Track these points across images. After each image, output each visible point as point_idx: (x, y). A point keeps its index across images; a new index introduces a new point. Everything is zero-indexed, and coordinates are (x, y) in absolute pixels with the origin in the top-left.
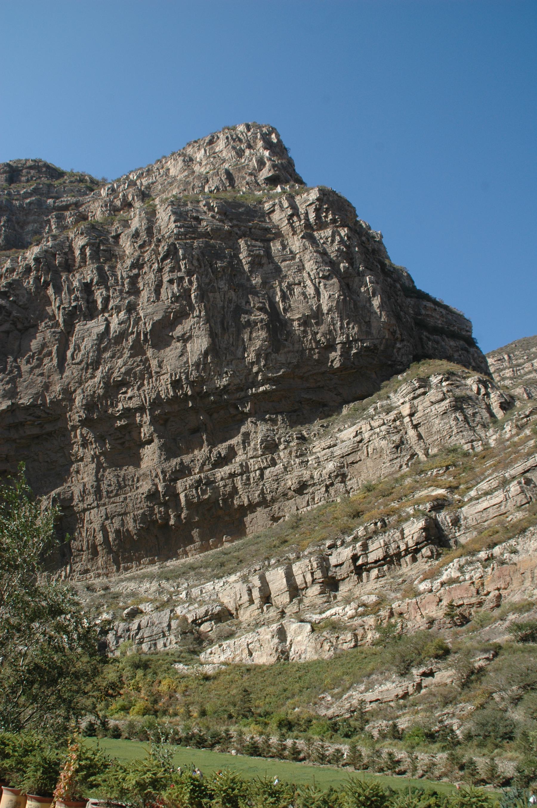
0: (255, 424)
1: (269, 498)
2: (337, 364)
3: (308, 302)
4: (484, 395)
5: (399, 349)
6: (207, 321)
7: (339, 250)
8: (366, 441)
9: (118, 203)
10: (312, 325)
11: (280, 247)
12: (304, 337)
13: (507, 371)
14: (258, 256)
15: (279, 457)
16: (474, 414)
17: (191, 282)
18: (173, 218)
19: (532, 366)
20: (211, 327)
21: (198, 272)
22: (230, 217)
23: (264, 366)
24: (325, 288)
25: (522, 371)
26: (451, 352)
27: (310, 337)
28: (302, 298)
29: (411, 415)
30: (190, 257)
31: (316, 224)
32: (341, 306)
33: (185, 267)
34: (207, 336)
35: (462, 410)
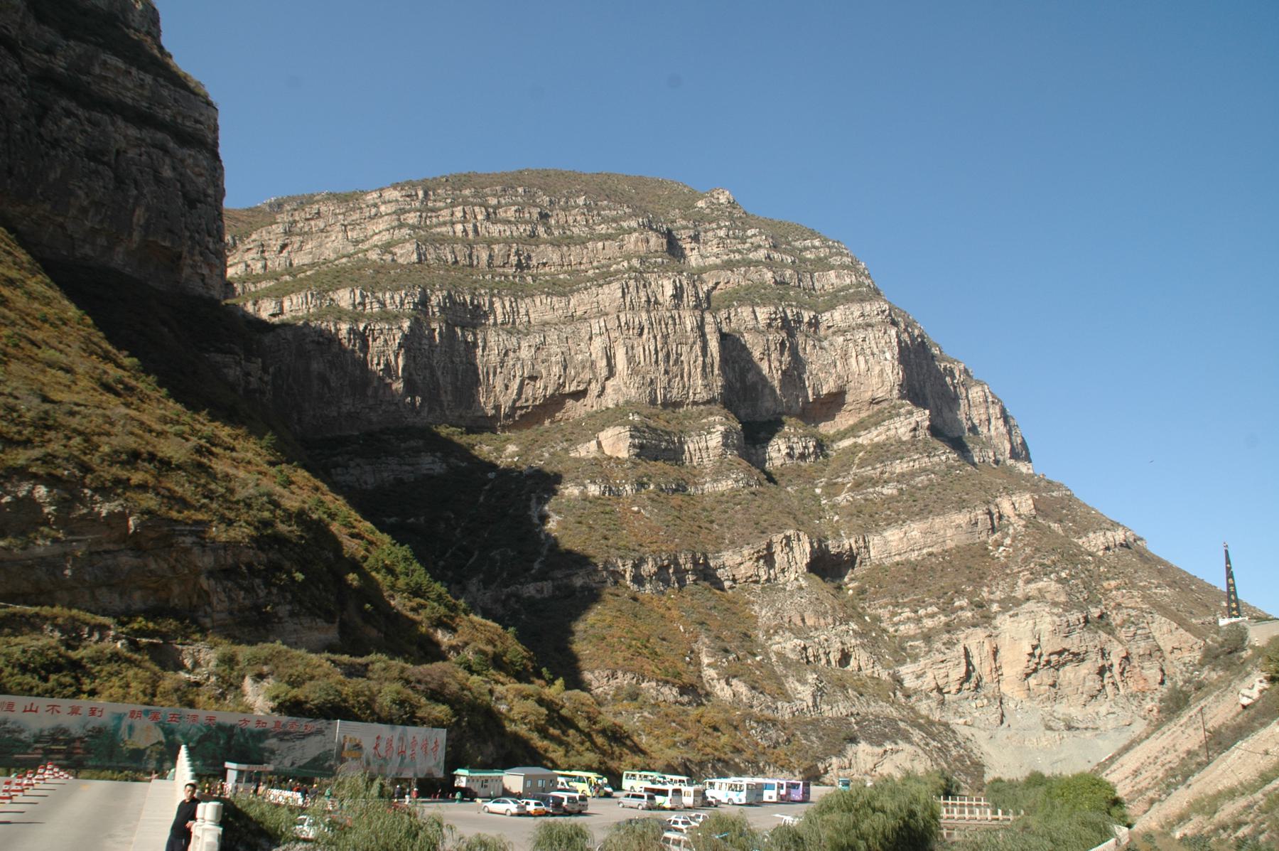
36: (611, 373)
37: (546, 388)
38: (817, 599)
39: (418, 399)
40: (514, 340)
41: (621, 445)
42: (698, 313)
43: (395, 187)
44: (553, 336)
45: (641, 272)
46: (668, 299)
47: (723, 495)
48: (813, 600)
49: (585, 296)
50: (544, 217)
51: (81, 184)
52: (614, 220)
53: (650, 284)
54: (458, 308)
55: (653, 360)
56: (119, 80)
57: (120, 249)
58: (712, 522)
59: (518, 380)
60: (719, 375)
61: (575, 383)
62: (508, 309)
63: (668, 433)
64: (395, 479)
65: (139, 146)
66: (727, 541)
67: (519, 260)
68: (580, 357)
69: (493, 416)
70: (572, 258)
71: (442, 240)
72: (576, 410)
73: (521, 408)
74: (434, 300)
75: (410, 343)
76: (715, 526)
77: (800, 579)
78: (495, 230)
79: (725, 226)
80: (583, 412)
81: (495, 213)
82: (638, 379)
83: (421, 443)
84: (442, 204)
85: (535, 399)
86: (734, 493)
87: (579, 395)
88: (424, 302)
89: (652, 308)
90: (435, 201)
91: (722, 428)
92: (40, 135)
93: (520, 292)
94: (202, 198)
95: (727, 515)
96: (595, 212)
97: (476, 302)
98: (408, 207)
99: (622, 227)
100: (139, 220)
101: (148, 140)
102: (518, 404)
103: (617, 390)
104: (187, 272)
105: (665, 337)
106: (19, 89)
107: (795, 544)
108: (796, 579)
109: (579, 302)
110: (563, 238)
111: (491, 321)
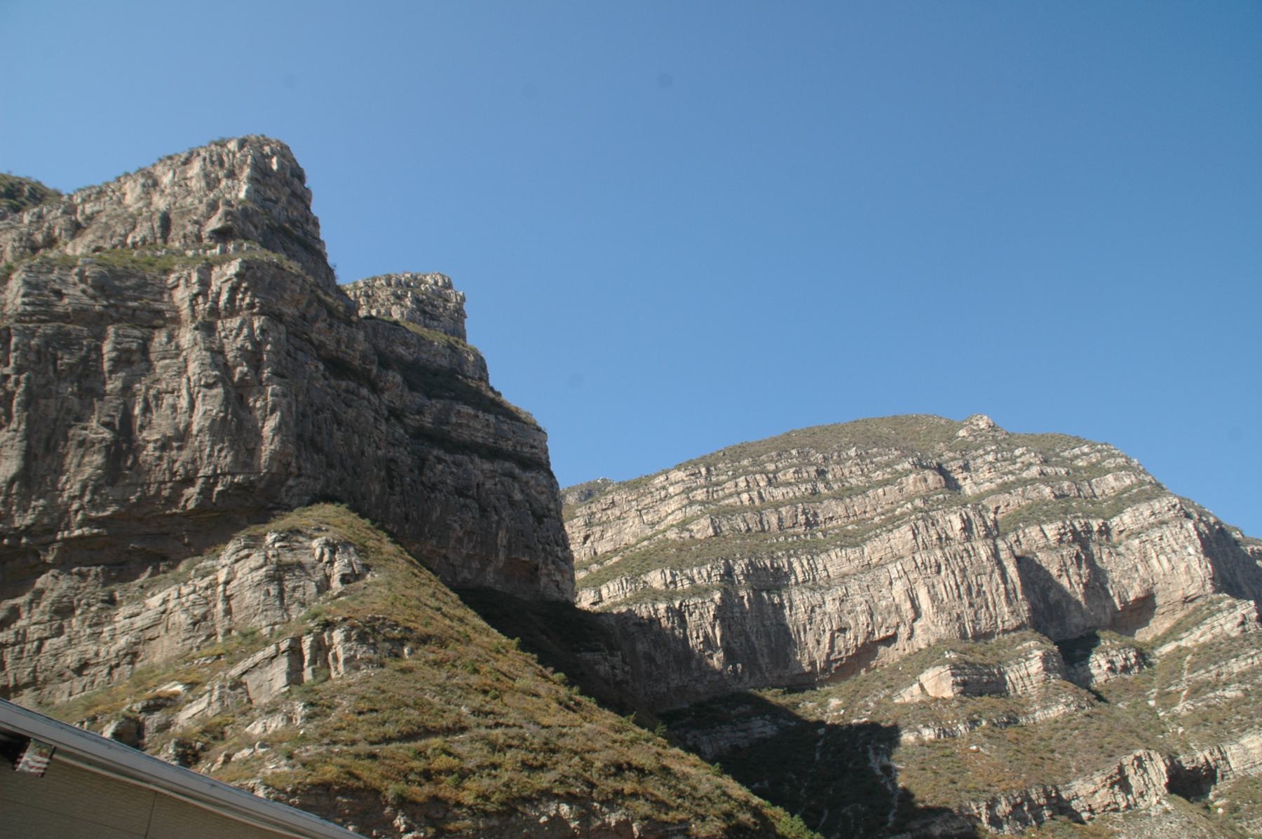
0: (56, 578)
1: (41, 678)
2: (191, 505)
3: (175, 418)
4: (327, 563)
5: (291, 487)
6: (27, 436)
7: (242, 348)
8: (168, 612)
9: (39, 237)
10: (172, 449)
11: (165, 340)
12: (157, 466)
13: (700, 491)
14: (129, 351)
15: (70, 626)
16: (294, 589)
17: (17, 383)
18: (22, 291)
19: (736, 486)
20: (29, 447)
21: (33, 370)
22: (108, 293)
23: (89, 502)
24: (204, 400)
25: (720, 493)
26: (481, 478)
27: (165, 466)
28: (169, 412)
29: (227, 583)
30: (26, 349)
31: (226, 308)
32: (216, 427)
33: (15, 363)
34: (20, 458)
35: (280, 581)
36: (917, 614)
37: (856, 638)
39: (739, 666)
40: (818, 596)
41: (944, 684)
42: (989, 541)
43: (678, 468)
44: (854, 586)
45: (926, 512)
46: (958, 533)
47: (1056, 722)
49: (877, 543)
50: (821, 473)
51: (456, 518)
52: (888, 465)
53: (938, 521)
54: (760, 573)
55: (956, 595)
56: (471, 424)
57: (490, 569)
58: (1052, 751)
59: (828, 634)
60: (1023, 599)
61: (883, 629)
62: (807, 567)
63: (986, 666)
64: (731, 746)
66: (1074, 770)
67: (807, 519)
68: (884, 603)
69: (810, 673)
70: (856, 508)
71: (731, 511)
72: (889, 656)
73: (836, 661)
74: (737, 570)
75: (725, 613)
76: (1057, 755)
78: (778, 493)
79: (992, 450)
80: (896, 657)
81: (775, 477)
82: (944, 616)
83: (749, 707)
84: (724, 478)
85: (847, 650)
86: (1068, 718)
87: (890, 640)
88: (729, 572)
89: (944, 545)
91: (1039, 653)
92: (422, 483)
93: (814, 549)
94: (547, 513)
95: (1066, 742)
96: (868, 461)
97: (776, 565)
98: (694, 485)
99: (897, 471)
102: (832, 657)
103: (926, 630)
104: (544, 580)
105: (963, 570)
107: (1147, 764)
109: (873, 550)
110: (843, 491)
111: (793, 581)
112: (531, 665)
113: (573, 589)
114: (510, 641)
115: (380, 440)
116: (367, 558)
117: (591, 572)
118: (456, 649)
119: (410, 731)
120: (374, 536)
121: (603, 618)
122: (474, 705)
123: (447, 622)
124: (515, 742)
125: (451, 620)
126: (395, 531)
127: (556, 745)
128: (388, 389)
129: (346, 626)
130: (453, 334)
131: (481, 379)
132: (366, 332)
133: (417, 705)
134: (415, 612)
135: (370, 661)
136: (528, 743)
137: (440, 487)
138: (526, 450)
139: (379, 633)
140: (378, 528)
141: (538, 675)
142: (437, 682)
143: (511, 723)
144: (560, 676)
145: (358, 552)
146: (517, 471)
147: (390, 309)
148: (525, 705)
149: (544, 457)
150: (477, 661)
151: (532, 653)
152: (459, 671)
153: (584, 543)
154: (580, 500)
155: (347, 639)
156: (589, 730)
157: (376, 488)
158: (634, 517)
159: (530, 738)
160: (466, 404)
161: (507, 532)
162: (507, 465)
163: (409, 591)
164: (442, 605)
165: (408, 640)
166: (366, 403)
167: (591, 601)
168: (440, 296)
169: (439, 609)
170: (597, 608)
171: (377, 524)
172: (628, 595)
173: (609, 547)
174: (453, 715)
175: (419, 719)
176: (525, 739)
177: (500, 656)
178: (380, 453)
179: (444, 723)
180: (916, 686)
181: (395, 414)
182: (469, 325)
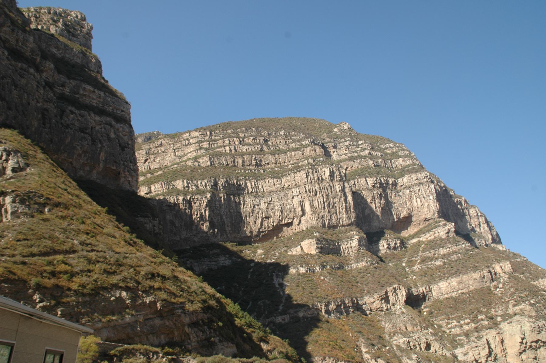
4: (4, 160)
36: (304, 213)
37: (273, 222)
38: (412, 318)
39: (216, 230)
40: (257, 200)
41: (312, 248)
42: (341, 183)
43: (196, 130)
44: (275, 197)
45: (314, 166)
46: (328, 177)
47: (361, 269)
48: (410, 318)
49: (288, 178)
50: (266, 141)
52: (298, 141)
53: (318, 171)
54: (231, 186)
55: (323, 206)
56: (91, 96)
57: (95, 172)
58: (357, 282)
59: (260, 219)
60: (353, 212)
61: (287, 219)
62: (254, 186)
63: (332, 241)
64: (208, 268)
65: (100, 125)
66: (366, 291)
67: (257, 162)
68: (288, 207)
69: (250, 236)
70: (280, 160)
71: (220, 155)
72: (288, 232)
73: (263, 232)
74: (220, 183)
75: (212, 204)
76: (359, 284)
77: (402, 308)
78: (244, 148)
79: (348, 140)
80: (291, 232)
81: (243, 140)
82: (316, 216)
83: (219, 250)
84: (218, 138)
85: (269, 227)
86: (366, 268)
87: (289, 225)
88: (216, 184)
89: (320, 182)
90: (215, 136)
91: (357, 237)
92: (62, 123)
93: (258, 177)
94: (127, 146)
95: (364, 279)
96: (289, 138)
97: (239, 183)
98: (203, 140)
99: (302, 144)
100: (102, 158)
101: (104, 122)
102: (261, 230)
103: (307, 221)
104: (122, 180)
105: (327, 195)
106: (54, 104)
107: (398, 291)
108: (400, 308)
109: (286, 181)
110: (275, 151)
111: (246, 192)
112: (112, 222)
113: (137, 185)
114: (102, 209)
115: (39, 97)
116: (28, 160)
117: (147, 177)
118: (73, 211)
119: (46, 251)
120: (33, 149)
121: (151, 201)
122: (81, 240)
123: (70, 196)
124: (101, 260)
125: (72, 196)
126: (44, 147)
127: (122, 262)
128: (45, 71)
129: (13, 195)
130: (85, 46)
131: (98, 72)
132: (34, 38)
133: (51, 238)
134: (53, 190)
135: (26, 214)
136: (108, 261)
137: (71, 126)
138: (119, 112)
139: (32, 200)
140: (35, 145)
141: (115, 227)
142: (62, 227)
143: (100, 249)
144: (127, 228)
145: (23, 156)
146: (113, 123)
147: (49, 27)
148: (108, 242)
149: (128, 117)
150: (84, 217)
151: (114, 215)
152: (74, 222)
153: (145, 163)
154: (145, 141)
155: (14, 201)
156: (139, 256)
157: (35, 123)
158: (171, 152)
159: (109, 258)
160: (89, 84)
161: (105, 153)
162: (108, 119)
163: (50, 179)
164: (68, 188)
165: (48, 204)
166: (32, 76)
167: (146, 192)
168: (79, 24)
169: (66, 190)
170: (148, 196)
171: (35, 143)
172: (164, 191)
173: (157, 166)
174: (70, 244)
175: (51, 245)
176: (106, 258)
177: (97, 216)
178: (39, 105)
179: (65, 248)
180: (299, 247)
181: (49, 85)
182: (94, 42)
